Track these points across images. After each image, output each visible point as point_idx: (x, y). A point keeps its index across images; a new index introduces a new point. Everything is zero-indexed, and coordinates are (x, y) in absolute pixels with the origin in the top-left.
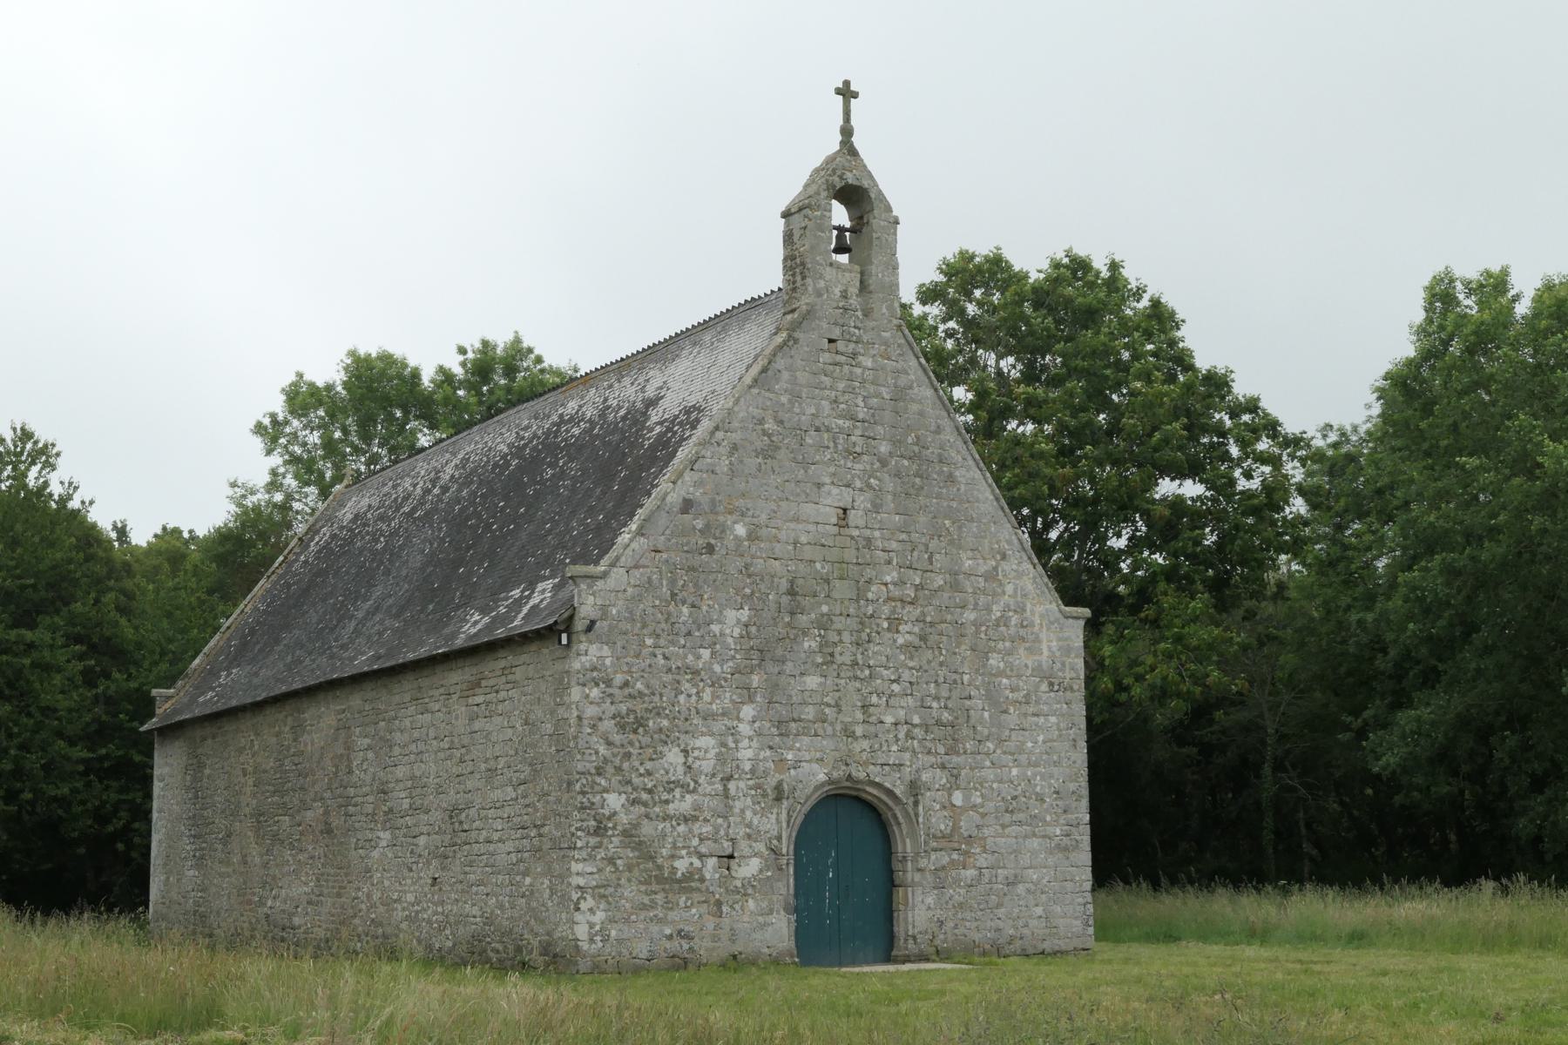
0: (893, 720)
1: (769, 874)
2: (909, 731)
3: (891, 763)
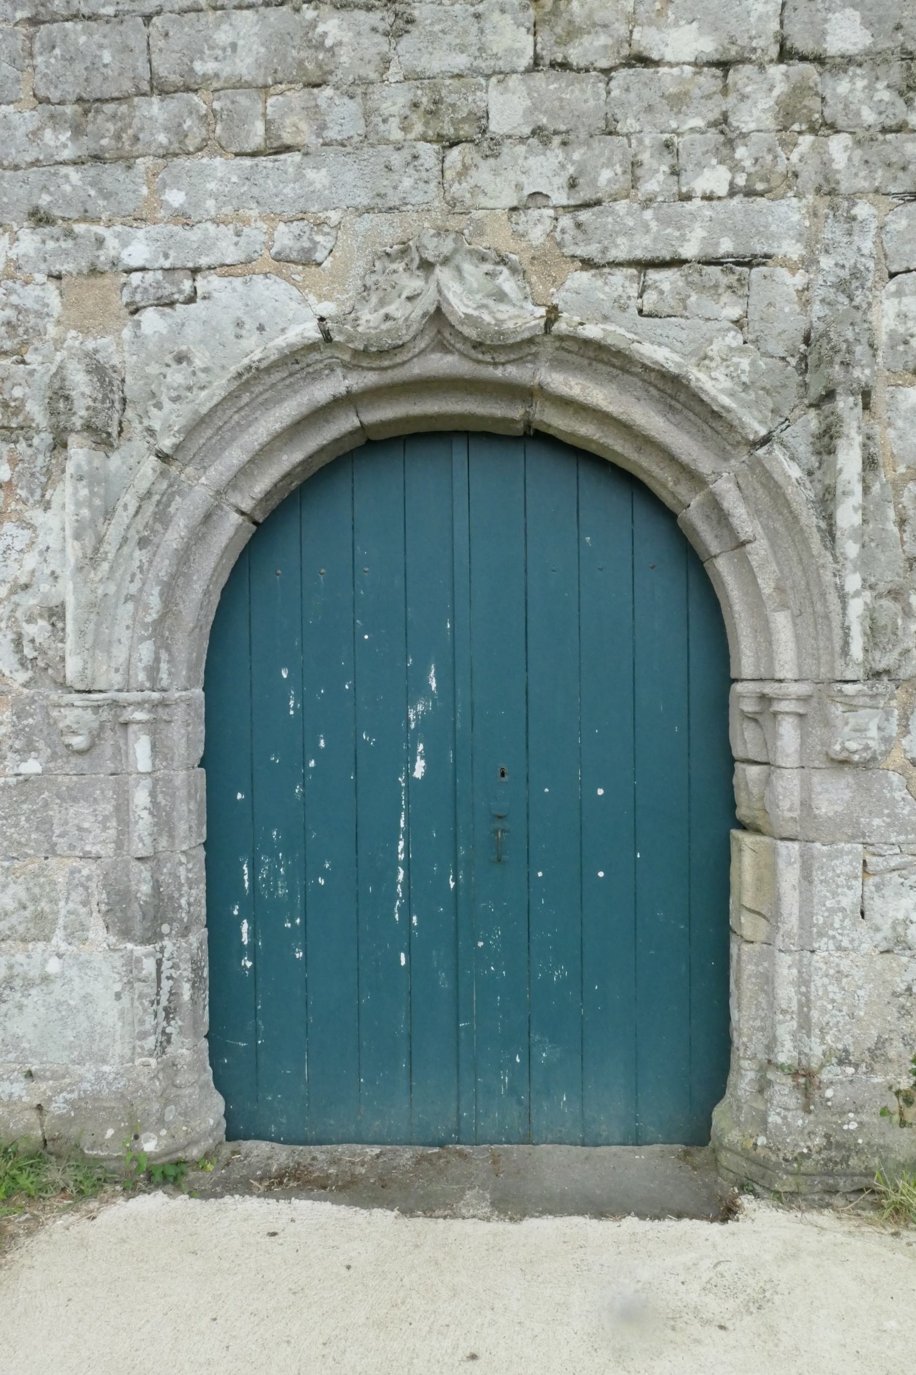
0: (708, 46)
1: (32, 766)
2: (800, 90)
3: (689, 251)
